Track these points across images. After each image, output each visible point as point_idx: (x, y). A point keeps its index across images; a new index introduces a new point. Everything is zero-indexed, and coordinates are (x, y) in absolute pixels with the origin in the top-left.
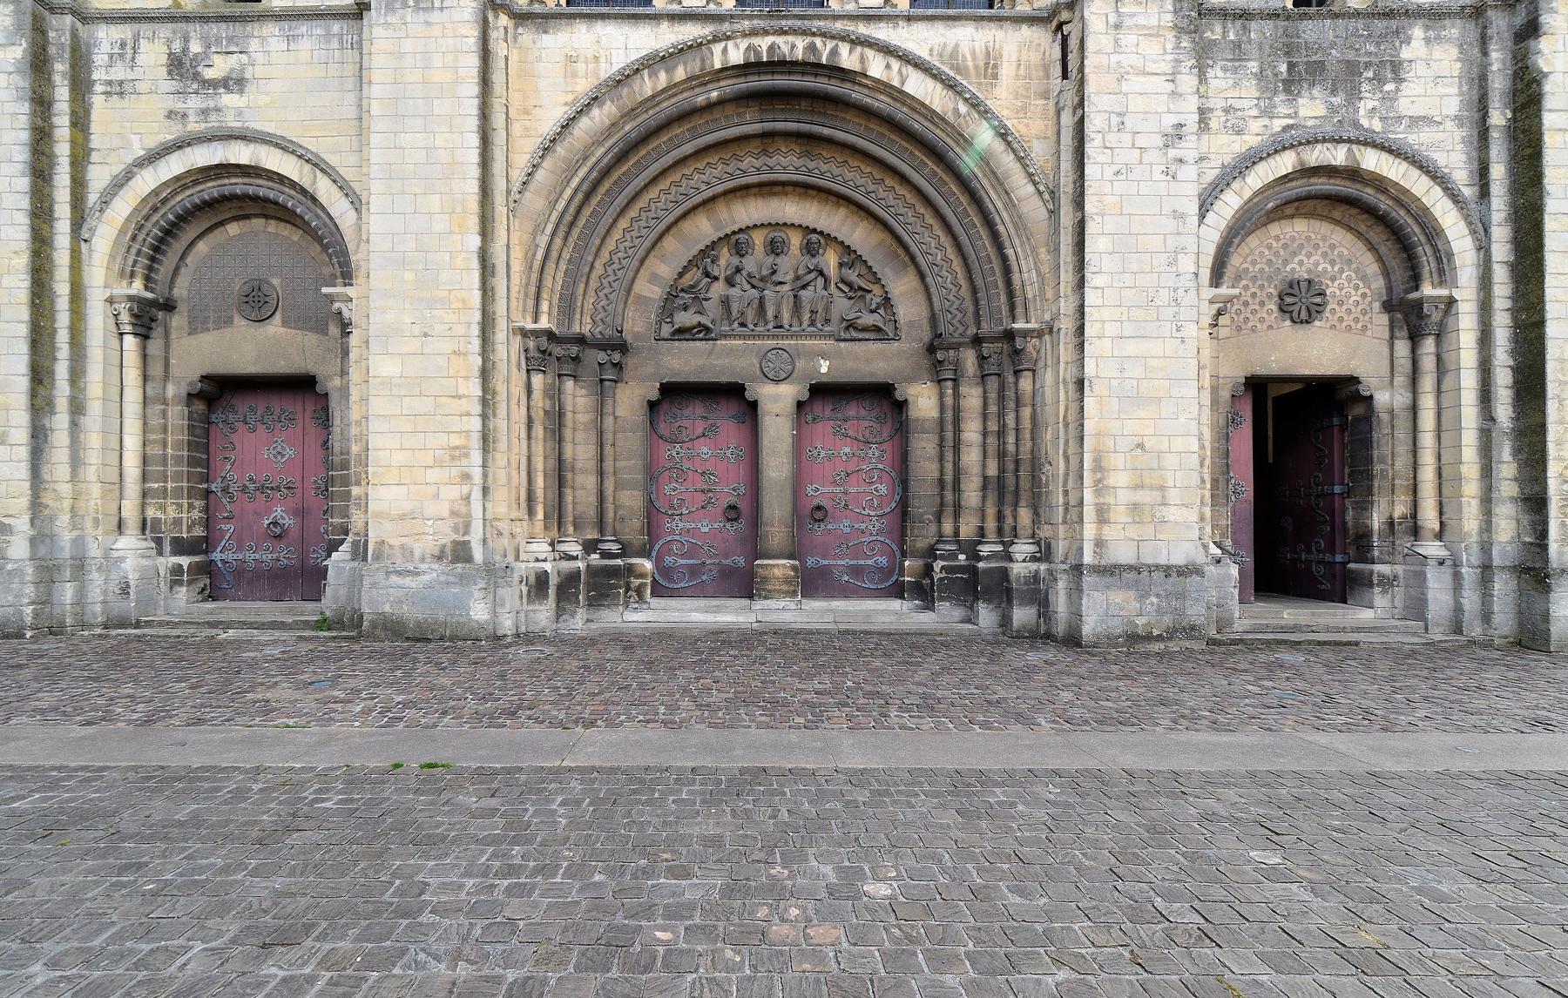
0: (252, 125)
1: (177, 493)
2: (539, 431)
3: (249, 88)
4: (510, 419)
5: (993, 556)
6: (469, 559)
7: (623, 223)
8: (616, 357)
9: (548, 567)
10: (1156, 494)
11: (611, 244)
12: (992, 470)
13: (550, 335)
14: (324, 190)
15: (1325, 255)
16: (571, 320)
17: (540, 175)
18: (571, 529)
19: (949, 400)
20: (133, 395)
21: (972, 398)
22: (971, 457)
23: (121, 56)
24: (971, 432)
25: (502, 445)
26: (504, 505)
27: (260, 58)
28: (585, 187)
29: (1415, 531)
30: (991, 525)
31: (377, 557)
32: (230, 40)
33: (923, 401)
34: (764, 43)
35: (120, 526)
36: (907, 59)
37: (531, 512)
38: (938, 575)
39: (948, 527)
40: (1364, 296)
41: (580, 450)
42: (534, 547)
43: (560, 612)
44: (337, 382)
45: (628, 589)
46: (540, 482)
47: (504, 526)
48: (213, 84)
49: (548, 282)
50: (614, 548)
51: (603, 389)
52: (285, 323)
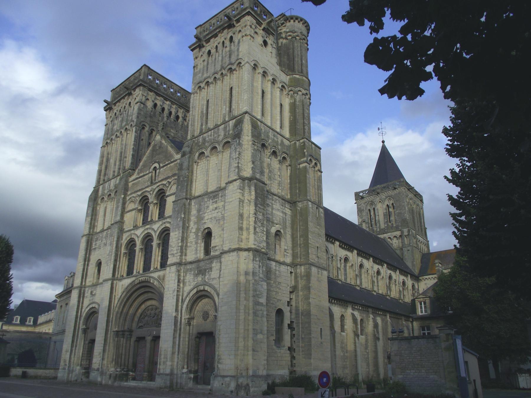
34: (141, 279)
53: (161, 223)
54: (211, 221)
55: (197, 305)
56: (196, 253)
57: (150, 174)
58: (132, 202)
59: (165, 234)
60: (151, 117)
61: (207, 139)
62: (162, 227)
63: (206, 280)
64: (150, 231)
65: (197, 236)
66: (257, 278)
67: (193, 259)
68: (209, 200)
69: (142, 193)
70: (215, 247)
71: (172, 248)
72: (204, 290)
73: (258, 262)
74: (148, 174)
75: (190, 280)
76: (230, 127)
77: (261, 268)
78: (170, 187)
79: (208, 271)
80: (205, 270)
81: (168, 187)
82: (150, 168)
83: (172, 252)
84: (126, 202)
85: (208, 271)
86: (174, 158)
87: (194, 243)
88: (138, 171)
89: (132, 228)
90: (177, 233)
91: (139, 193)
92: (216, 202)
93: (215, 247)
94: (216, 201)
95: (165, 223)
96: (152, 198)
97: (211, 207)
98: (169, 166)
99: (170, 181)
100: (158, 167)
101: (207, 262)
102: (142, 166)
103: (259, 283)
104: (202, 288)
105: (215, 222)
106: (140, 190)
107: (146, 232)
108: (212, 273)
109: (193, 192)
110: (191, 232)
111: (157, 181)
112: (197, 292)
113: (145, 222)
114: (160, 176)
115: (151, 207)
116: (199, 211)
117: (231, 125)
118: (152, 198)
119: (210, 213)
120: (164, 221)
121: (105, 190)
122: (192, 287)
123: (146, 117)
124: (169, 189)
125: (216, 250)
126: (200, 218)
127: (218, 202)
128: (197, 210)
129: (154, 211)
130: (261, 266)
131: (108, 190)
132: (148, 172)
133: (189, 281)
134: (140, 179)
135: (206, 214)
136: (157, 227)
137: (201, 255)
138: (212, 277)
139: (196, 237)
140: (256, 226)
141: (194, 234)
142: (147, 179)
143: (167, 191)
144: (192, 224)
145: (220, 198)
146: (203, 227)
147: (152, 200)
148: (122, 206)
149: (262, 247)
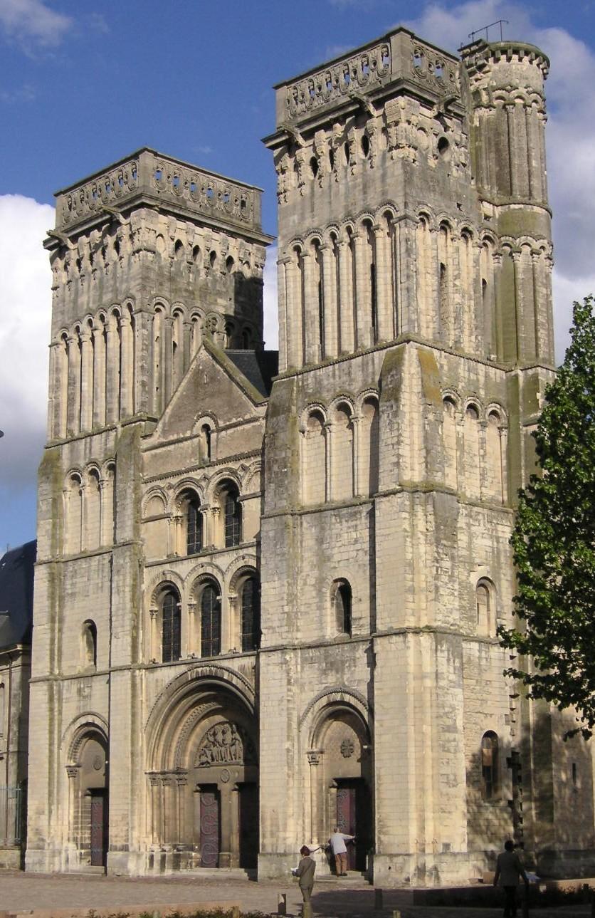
53: (231, 557)
54: (347, 567)
55: (328, 727)
56: (321, 628)
57: (196, 440)
58: (156, 499)
59: (251, 582)
60: (171, 279)
61: (325, 382)
63: (346, 683)
64: (209, 570)
65: (320, 593)
66: (442, 683)
67: (314, 639)
68: (341, 522)
69: (181, 483)
70: (360, 618)
71: (269, 616)
72: (342, 702)
73: (446, 653)
74: (190, 438)
75: (313, 680)
76: (376, 366)
77: (452, 663)
78: (247, 478)
79: (347, 665)
80: (343, 663)
82: (193, 426)
83: (270, 624)
84: (142, 497)
85: (347, 665)
86: (249, 411)
87: (314, 606)
88: (164, 427)
89: (165, 558)
90: (277, 584)
91: (174, 481)
93: (360, 618)
94: (356, 526)
96: (209, 498)
98: (239, 428)
100: (213, 427)
101: (346, 647)
102: (171, 416)
103: (449, 692)
104: (338, 697)
105: (357, 567)
106: (174, 474)
107: (201, 571)
108: (357, 669)
111: (213, 459)
112: (330, 704)
113: (195, 546)
114: (220, 448)
115: (208, 517)
116: (320, 541)
117: (376, 361)
119: (343, 549)
120: (241, 553)
121: (78, 458)
122: (316, 693)
123: (161, 284)
125: (362, 626)
126: (323, 559)
127: (359, 527)
128: (317, 540)
129: (215, 530)
130: (452, 660)
131: (87, 461)
132: (188, 434)
133: (310, 683)
134: (171, 448)
135: (336, 550)
136: (227, 565)
137: (331, 630)
138: (357, 677)
139: (317, 594)
140: (439, 583)
141: (312, 588)
142: (190, 451)
144: (306, 567)
148: (134, 508)
149: (452, 622)
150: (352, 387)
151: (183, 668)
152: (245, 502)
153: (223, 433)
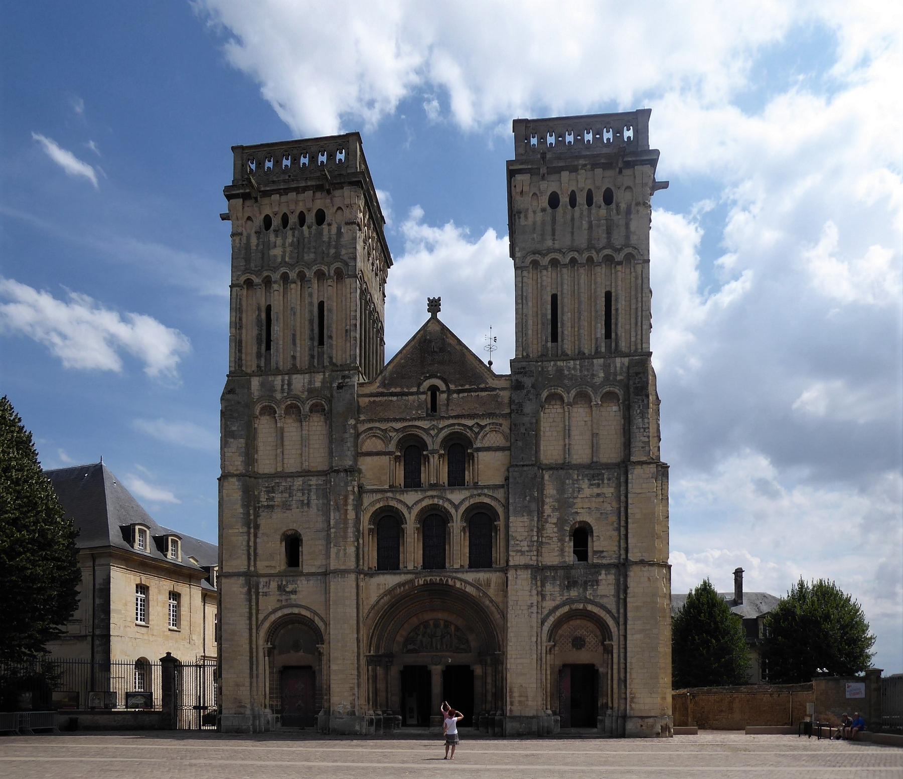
0: (299, 603)
1: (277, 697)
2: (371, 681)
3: (298, 593)
4: (364, 678)
5: (493, 714)
6: (355, 715)
7: (393, 622)
8: (391, 659)
9: (373, 717)
10: (525, 699)
11: (389, 628)
12: (494, 690)
13: (373, 656)
14: (317, 620)
15: (585, 630)
16: (379, 651)
17: (371, 615)
18: (379, 707)
19: (484, 670)
20: (267, 672)
21: (489, 670)
22: (489, 687)
23: (266, 585)
24: (489, 680)
25: (362, 686)
26: (363, 701)
27: (300, 585)
28: (382, 617)
29: (607, 707)
30: (493, 706)
31: (333, 714)
32: (293, 581)
33: (478, 670)
35: (265, 707)
36: (466, 582)
37: (369, 703)
38: (480, 720)
39: (484, 706)
40: (596, 641)
41: (381, 686)
42: (369, 712)
43: (376, 730)
44: (317, 668)
45: (395, 724)
46: (371, 695)
47: (363, 707)
48: (289, 592)
49: (373, 643)
50: (391, 712)
51: (387, 669)
52: (304, 652)
61: (566, 372)
62: (472, 501)
78: (481, 434)
81: (477, 434)
92: (598, 485)
95: (479, 495)
97: (587, 492)
99: (483, 423)
109: (542, 457)
110: (547, 522)
118: (433, 443)
120: (475, 492)
124: (480, 437)
143: (476, 438)
145: (606, 481)
146: (574, 519)
147: (437, 447)
150: (595, 381)
151: (409, 577)
152: (480, 453)
153: (455, 396)
